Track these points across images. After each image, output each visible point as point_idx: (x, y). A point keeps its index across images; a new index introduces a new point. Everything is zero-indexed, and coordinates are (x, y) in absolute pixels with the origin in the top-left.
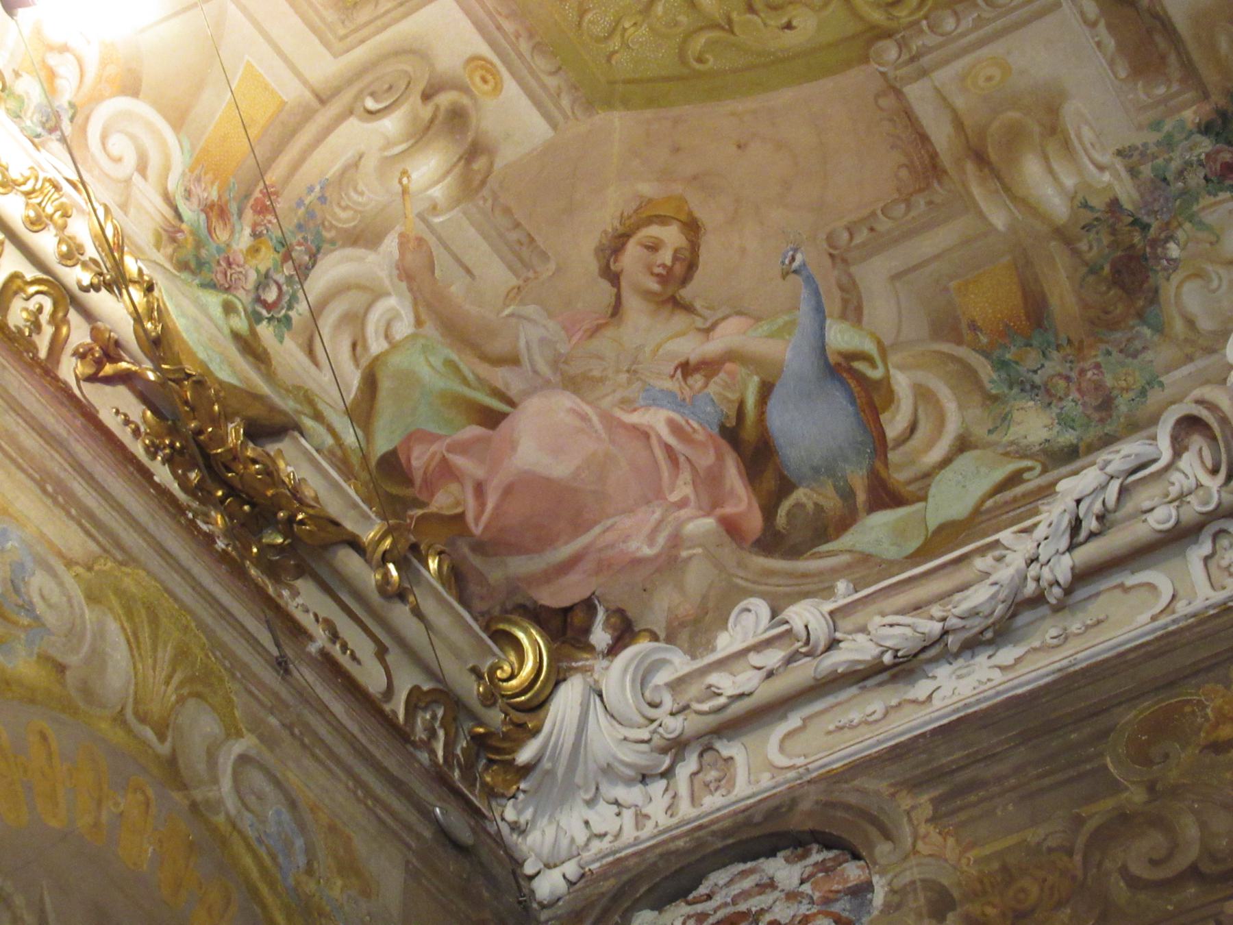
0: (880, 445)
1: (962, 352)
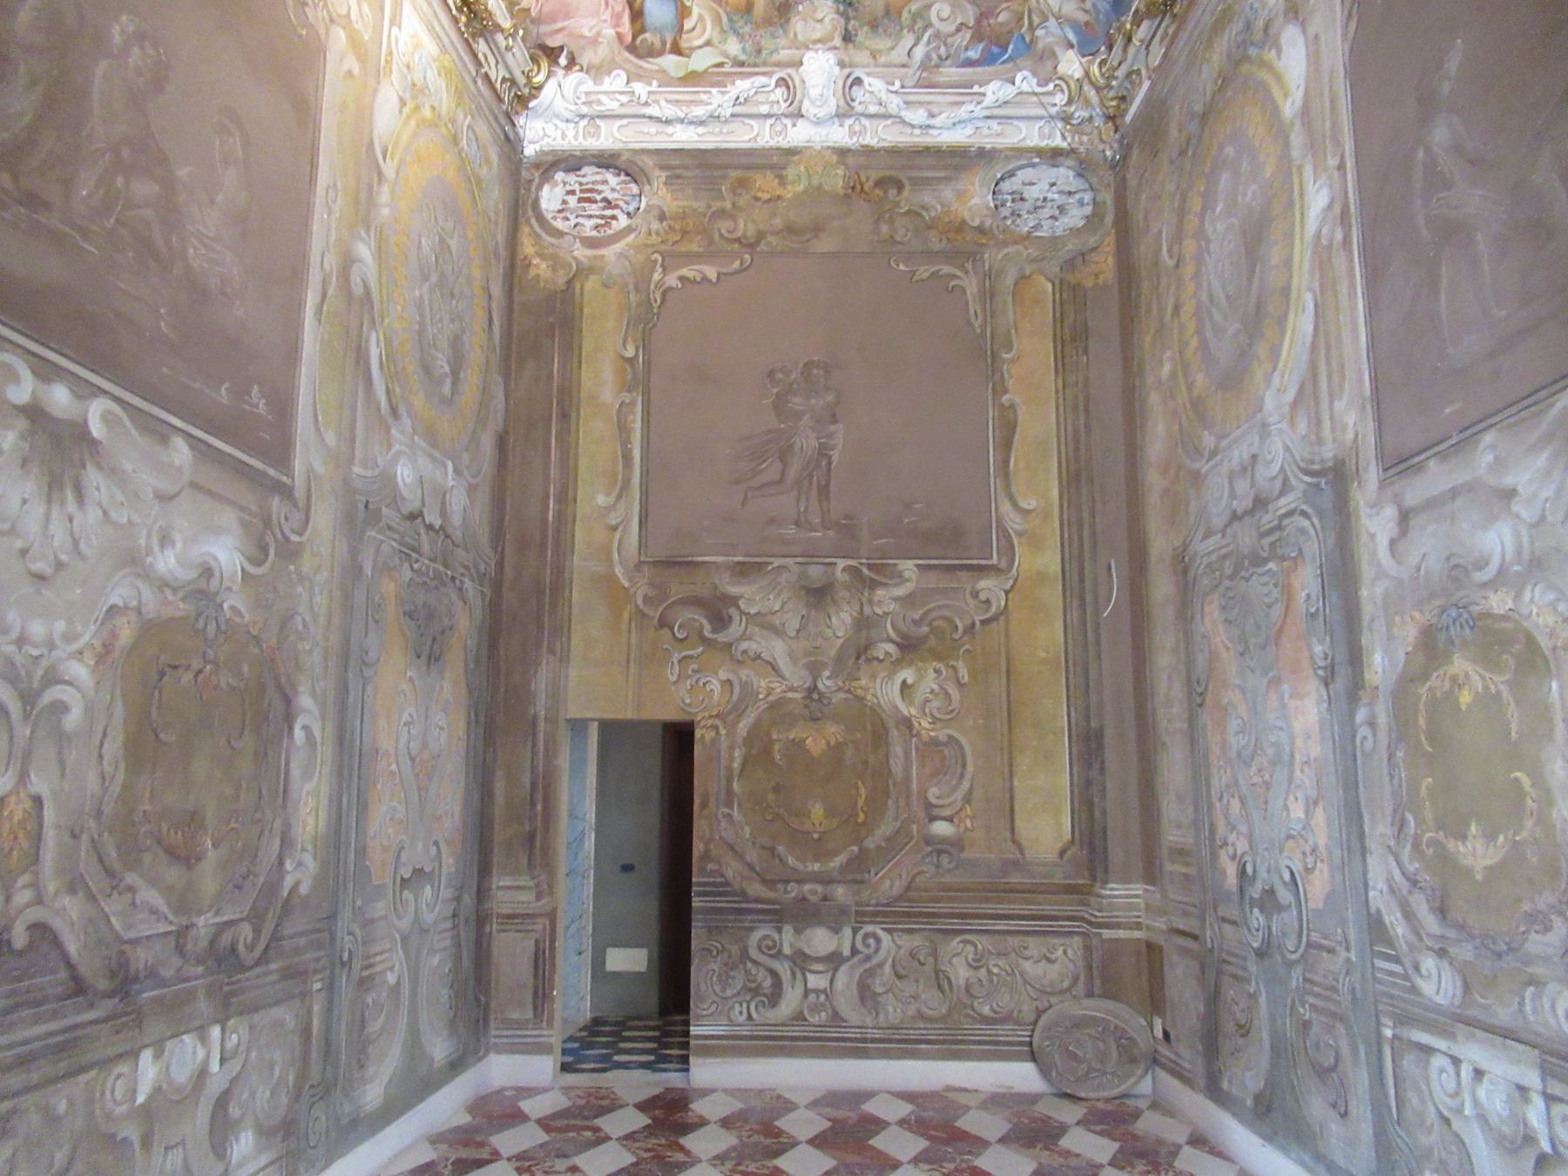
0: (681, 29)
1: (720, 10)
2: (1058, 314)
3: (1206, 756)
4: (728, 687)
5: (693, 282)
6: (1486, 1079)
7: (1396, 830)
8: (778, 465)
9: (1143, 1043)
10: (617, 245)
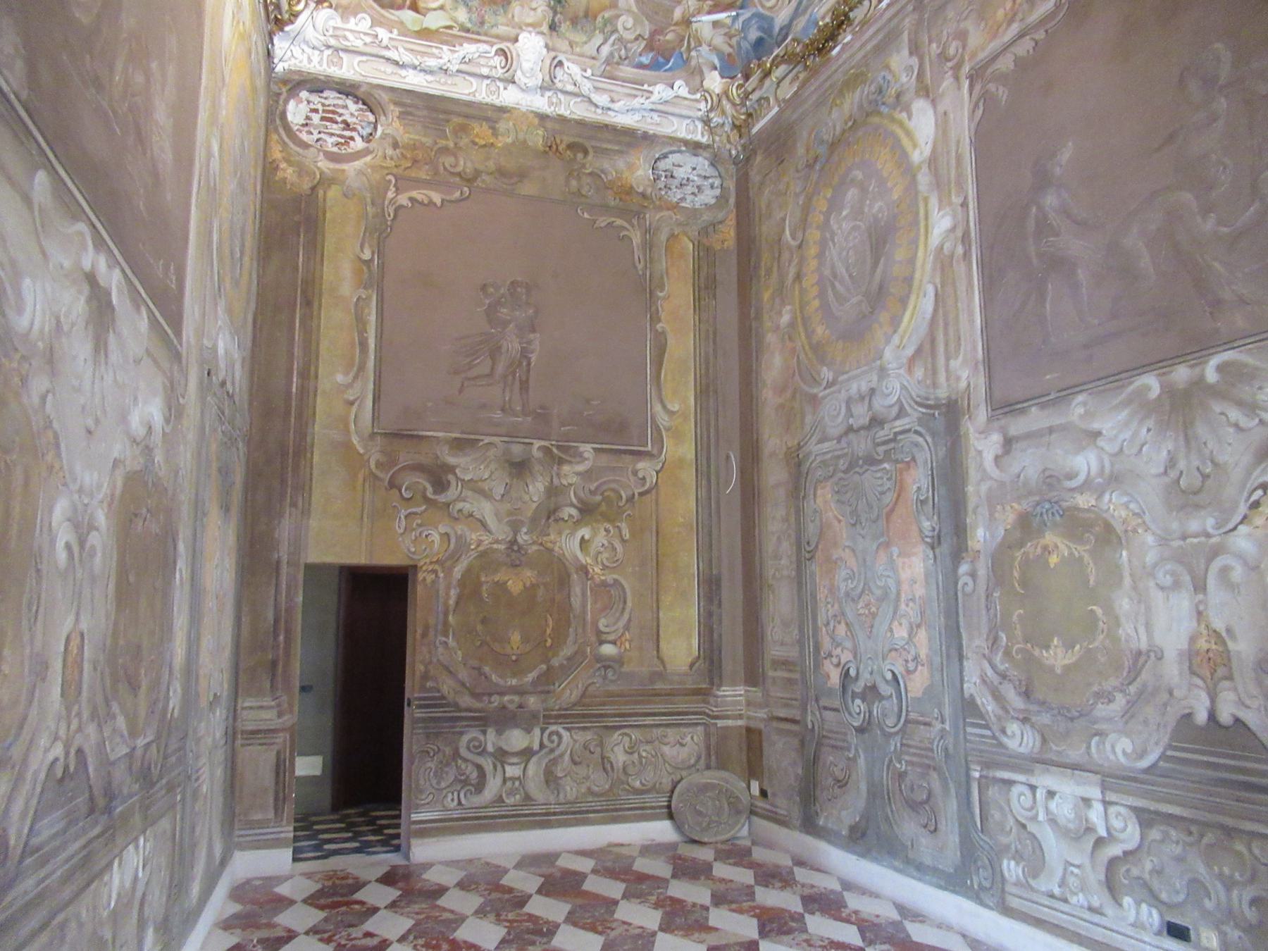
2: (696, 266)
3: (814, 596)
4: (445, 538)
5: (422, 203)
6: (1057, 797)
7: (990, 642)
8: (489, 362)
9: (745, 799)
10: (357, 163)
